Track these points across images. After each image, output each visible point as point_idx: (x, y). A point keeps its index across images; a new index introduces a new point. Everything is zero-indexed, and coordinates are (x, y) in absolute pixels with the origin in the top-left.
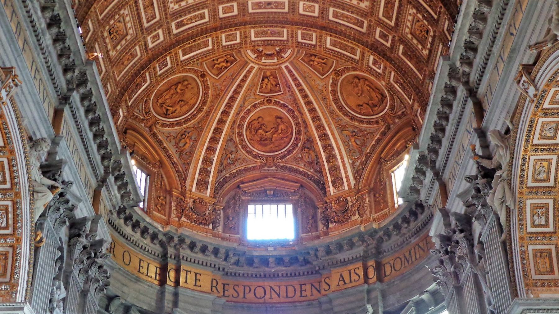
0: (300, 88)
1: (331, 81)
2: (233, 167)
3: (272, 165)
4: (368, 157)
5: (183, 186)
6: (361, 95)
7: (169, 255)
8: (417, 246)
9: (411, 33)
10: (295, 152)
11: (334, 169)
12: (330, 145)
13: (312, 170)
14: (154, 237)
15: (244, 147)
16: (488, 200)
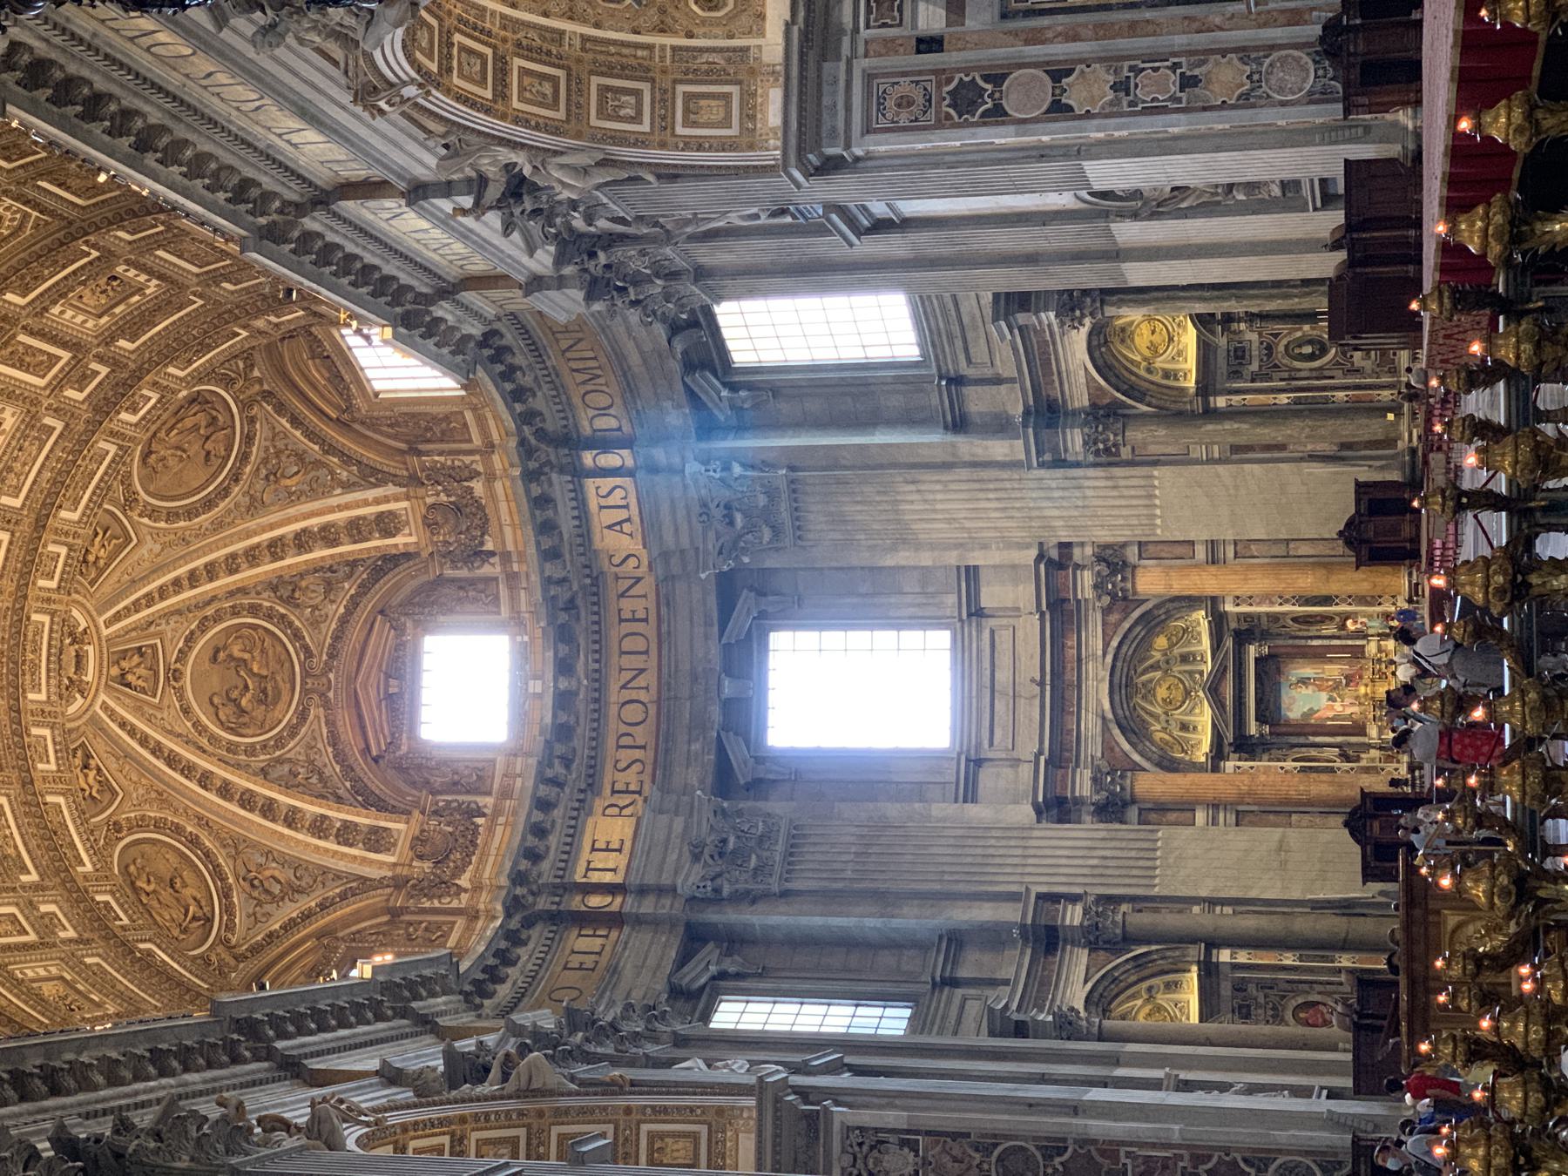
0: (157, 596)
1: (145, 520)
2: (328, 772)
3: (324, 680)
4: (330, 449)
5: (380, 883)
6: (184, 451)
7: (554, 907)
8: (568, 355)
9: (100, 316)
10: (297, 623)
11: (356, 529)
12: (298, 536)
13: (346, 585)
14: (514, 938)
15: (279, 742)
16: (566, 194)
